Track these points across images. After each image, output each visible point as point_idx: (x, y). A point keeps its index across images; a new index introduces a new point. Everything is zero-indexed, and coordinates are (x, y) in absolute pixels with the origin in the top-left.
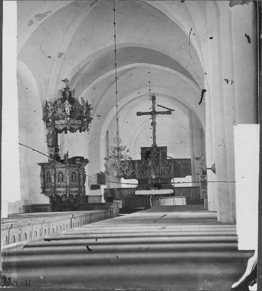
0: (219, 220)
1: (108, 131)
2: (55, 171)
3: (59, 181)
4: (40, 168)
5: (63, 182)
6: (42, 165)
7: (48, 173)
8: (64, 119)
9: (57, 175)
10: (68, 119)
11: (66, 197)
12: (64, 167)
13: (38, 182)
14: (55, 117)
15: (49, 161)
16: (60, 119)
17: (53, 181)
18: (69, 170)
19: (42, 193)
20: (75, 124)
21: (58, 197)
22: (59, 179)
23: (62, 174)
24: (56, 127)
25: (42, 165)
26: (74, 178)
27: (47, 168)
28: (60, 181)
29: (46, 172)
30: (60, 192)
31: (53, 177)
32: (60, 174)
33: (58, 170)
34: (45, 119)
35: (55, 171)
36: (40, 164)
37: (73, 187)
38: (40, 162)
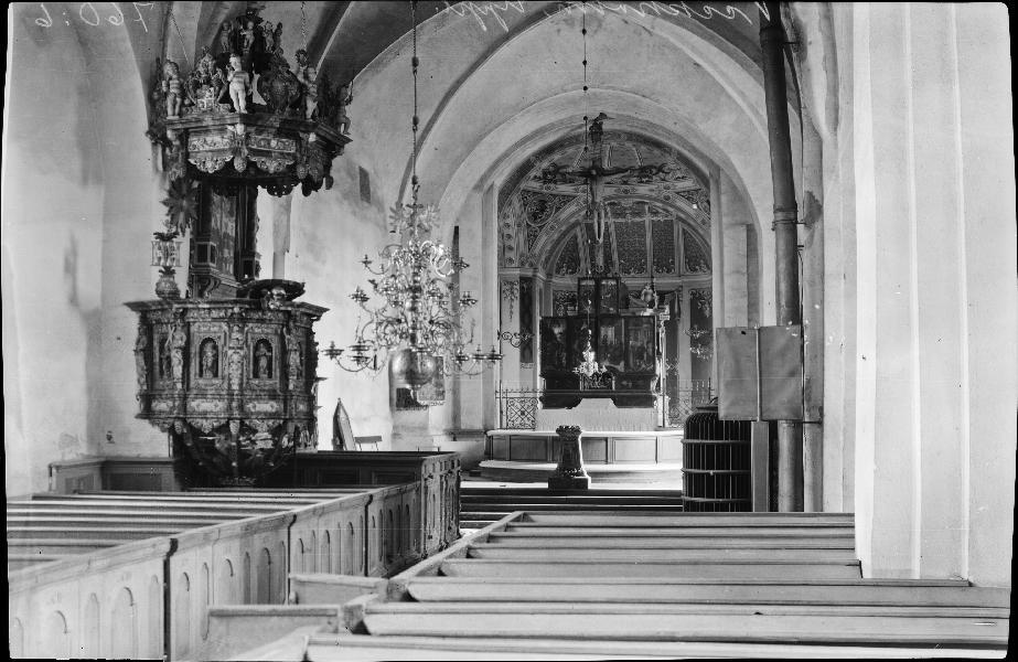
0: (868, 575)
1: (457, 228)
2: (188, 334)
3: (201, 371)
4: (133, 319)
5: (216, 375)
6: (141, 308)
7: (163, 341)
8: (222, 130)
9: (195, 349)
10: (240, 129)
11: (229, 435)
12: (221, 319)
13: (128, 380)
14: (189, 121)
15: (159, 293)
16: (206, 130)
17: (178, 371)
18: (241, 330)
19: (140, 416)
20: (267, 154)
21: (196, 432)
22: (201, 366)
23: (215, 348)
24: (192, 161)
25: (141, 308)
26: (263, 362)
27: (159, 322)
28: (208, 374)
29: (156, 336)
30: (204, 415)
31: (177, 357)
32: (209, 347)
33: (200, 330)
34: (157, 134)
35: (188, 334)
36: (134, 306)
37: (258, 398)
38: (132, 299)
